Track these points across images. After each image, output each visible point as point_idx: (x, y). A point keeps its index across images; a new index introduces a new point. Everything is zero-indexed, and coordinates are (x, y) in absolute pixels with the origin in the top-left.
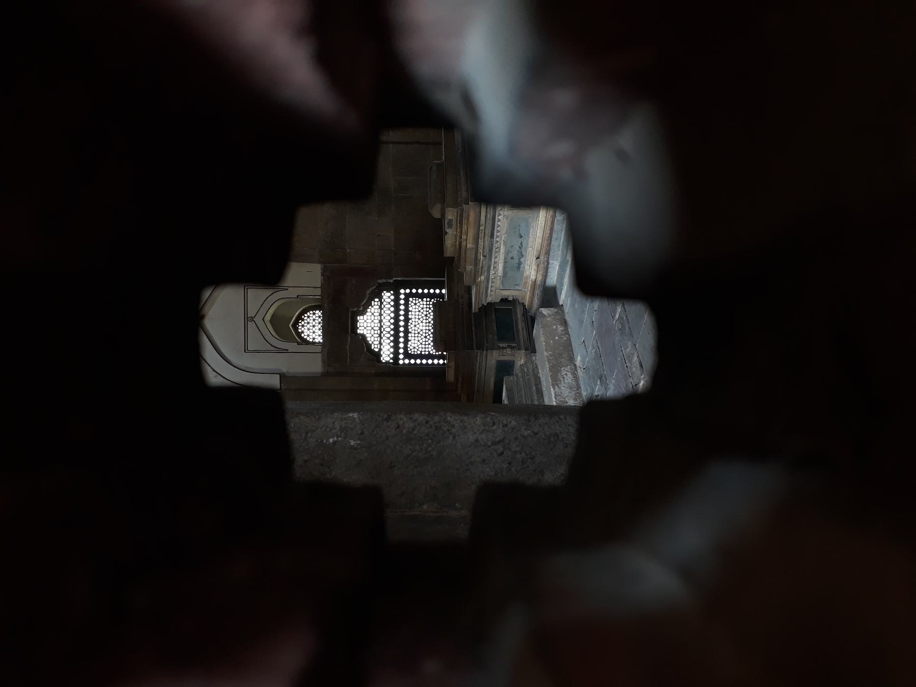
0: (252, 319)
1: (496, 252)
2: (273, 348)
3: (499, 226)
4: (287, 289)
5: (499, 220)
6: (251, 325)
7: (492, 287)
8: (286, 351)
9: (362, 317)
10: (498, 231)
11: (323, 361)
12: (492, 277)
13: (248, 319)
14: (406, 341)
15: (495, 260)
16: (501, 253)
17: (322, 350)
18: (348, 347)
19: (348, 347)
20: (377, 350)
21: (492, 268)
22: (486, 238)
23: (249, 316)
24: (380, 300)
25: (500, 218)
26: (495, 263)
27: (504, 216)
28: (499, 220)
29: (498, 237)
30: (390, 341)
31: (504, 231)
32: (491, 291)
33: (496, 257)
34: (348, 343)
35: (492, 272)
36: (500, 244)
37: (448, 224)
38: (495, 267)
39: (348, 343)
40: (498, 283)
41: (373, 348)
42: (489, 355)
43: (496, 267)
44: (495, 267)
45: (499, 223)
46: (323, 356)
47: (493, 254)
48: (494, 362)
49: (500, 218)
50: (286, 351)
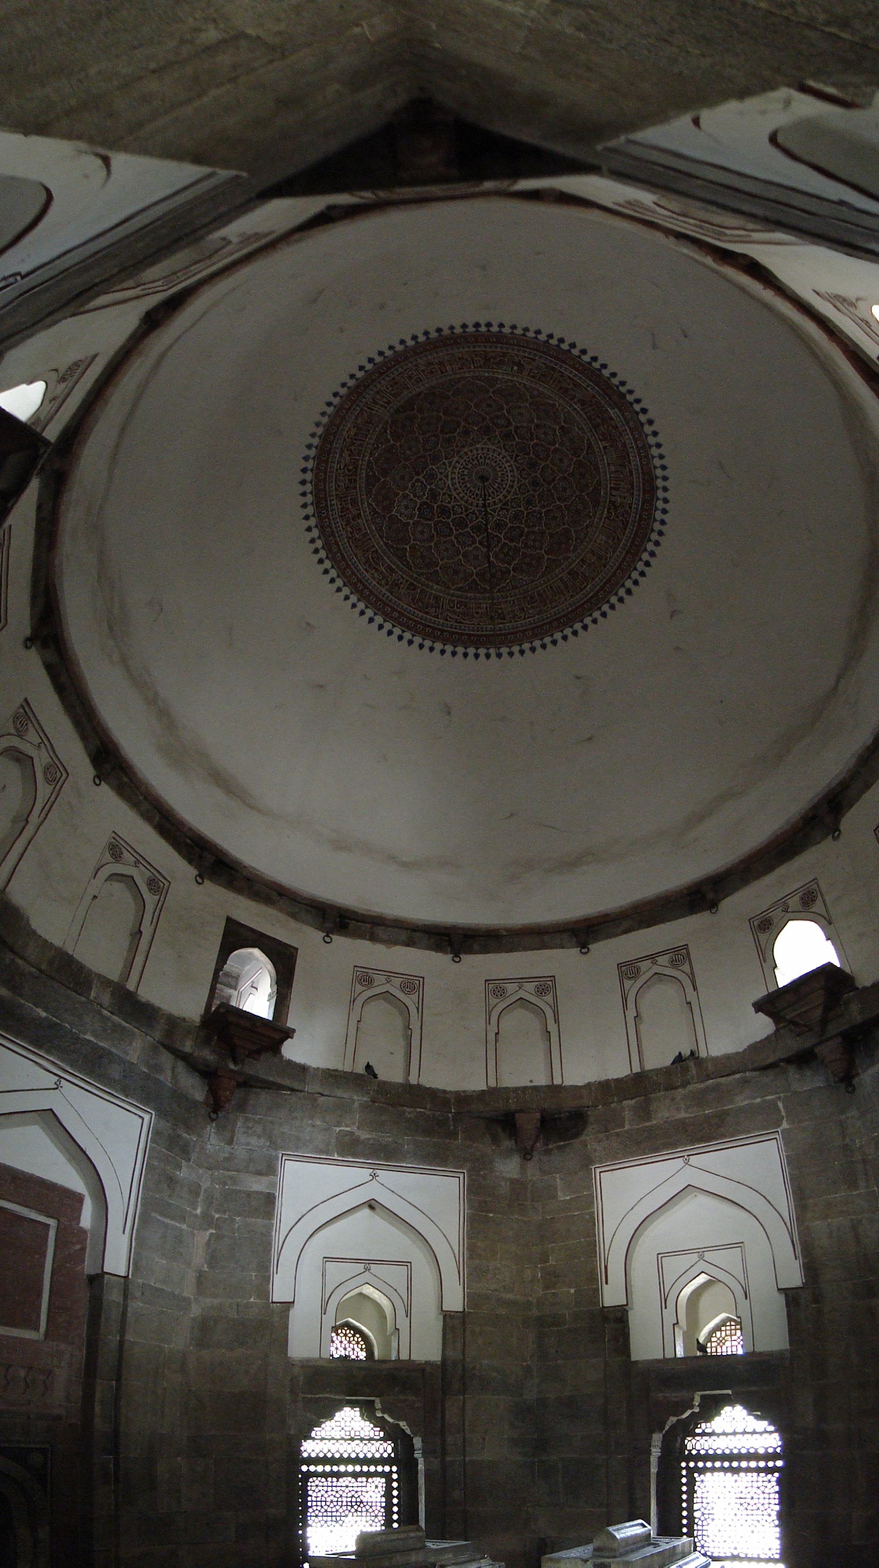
0: (367, 1269)
2: (327, 1296)
4: (407, 1316)
6: (360, 1267)
8: (324, 1311)
9: (358, 1413)
11: (308, 1360)
13: (368, 1263)
14: (324, 1475)
17: (322, 1359)
18: (327, 1395)
19: (327, 1395)
20: (313, 1434)
23: (371, 1265)
24: (381, 1439)
30: (325, 1452)
34: (332, 1396)
39: (332, 1396)
41: (315, 1429)
46: (316, 1360)
50: (324, 1311)
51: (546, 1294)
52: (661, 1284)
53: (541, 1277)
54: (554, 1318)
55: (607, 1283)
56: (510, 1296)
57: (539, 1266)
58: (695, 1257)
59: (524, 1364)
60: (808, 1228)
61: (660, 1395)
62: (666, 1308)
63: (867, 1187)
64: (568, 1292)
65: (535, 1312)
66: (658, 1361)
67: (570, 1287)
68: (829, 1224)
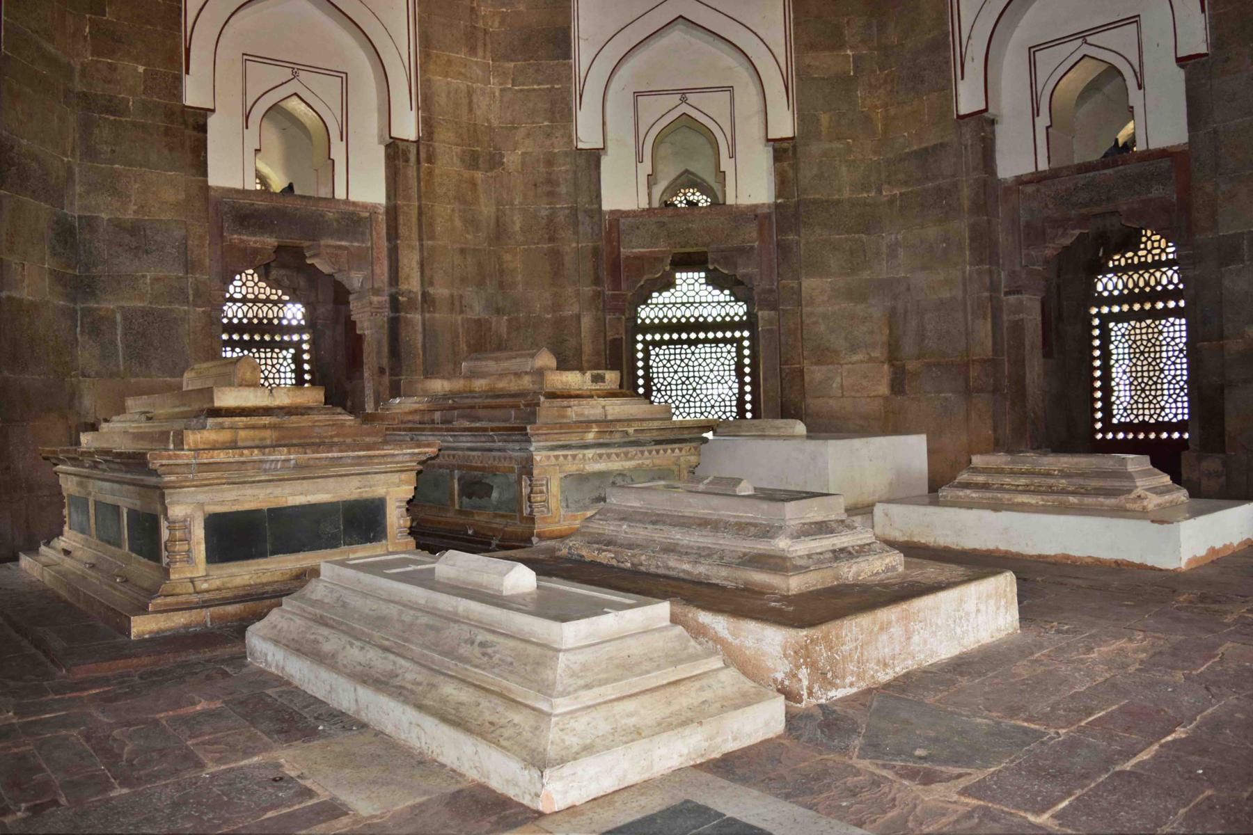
1: (626, 454)
3: (665, 451)
5: (673, 450)
7: (565, 457)
10: (658, 452)
12: (580, 453)
15: (614, 456)
16: (624, 463)
21: (599, 451)
22: (655, 433)
25: (677, 451)
26: (609, 456)
27: (679, 458)
28: (673, 450)
29: (650, 452)
31: (657, 462)
32: (557, 457)
33: (618, 455)
35: (590, 453)
36: (640, 459)
37: (598, 374)
38: (600, 456)
40: (572, 468)
42: (404, 476)
43: (601, 458)
44: (600, 456)
45: (669, 451)
47: (624, 449)
48: (379, 491)
49: (677, 451)
51: (97, 62)
52: (245, 94)
53: (90, 32)
54: (110, 101)
55: (187, 72)
56: (50, 48)
57: (87, 16)
58: (287, 74)
59: (65, 159)
60: (429, 80)
61: (235, 236)
62: (247, 128)
63: (484, 58)
64: (135, 69)
65: (78, 86)
66: (237, 191)
67: (137, 60)
68: (448, 83)
